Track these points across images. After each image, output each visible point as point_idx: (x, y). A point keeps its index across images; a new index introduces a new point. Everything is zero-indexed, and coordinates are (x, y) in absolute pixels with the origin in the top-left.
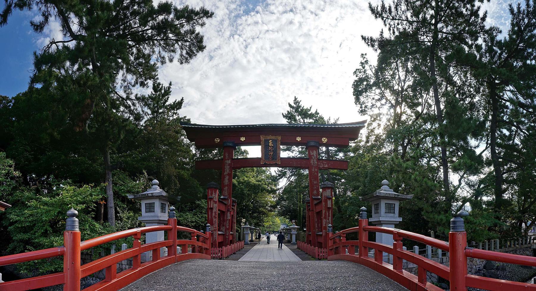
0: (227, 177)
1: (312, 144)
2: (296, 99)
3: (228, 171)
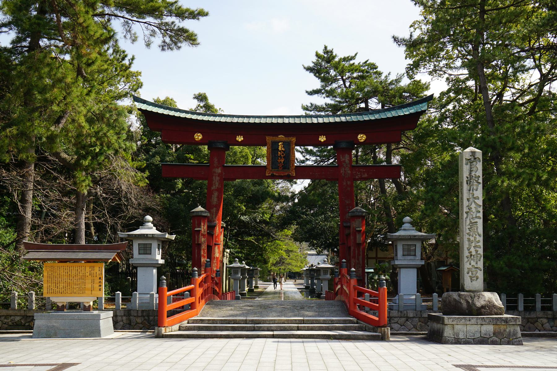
0: (216, 194)
1: (343, 145)
2: (326, 48)
3: (217, 184)
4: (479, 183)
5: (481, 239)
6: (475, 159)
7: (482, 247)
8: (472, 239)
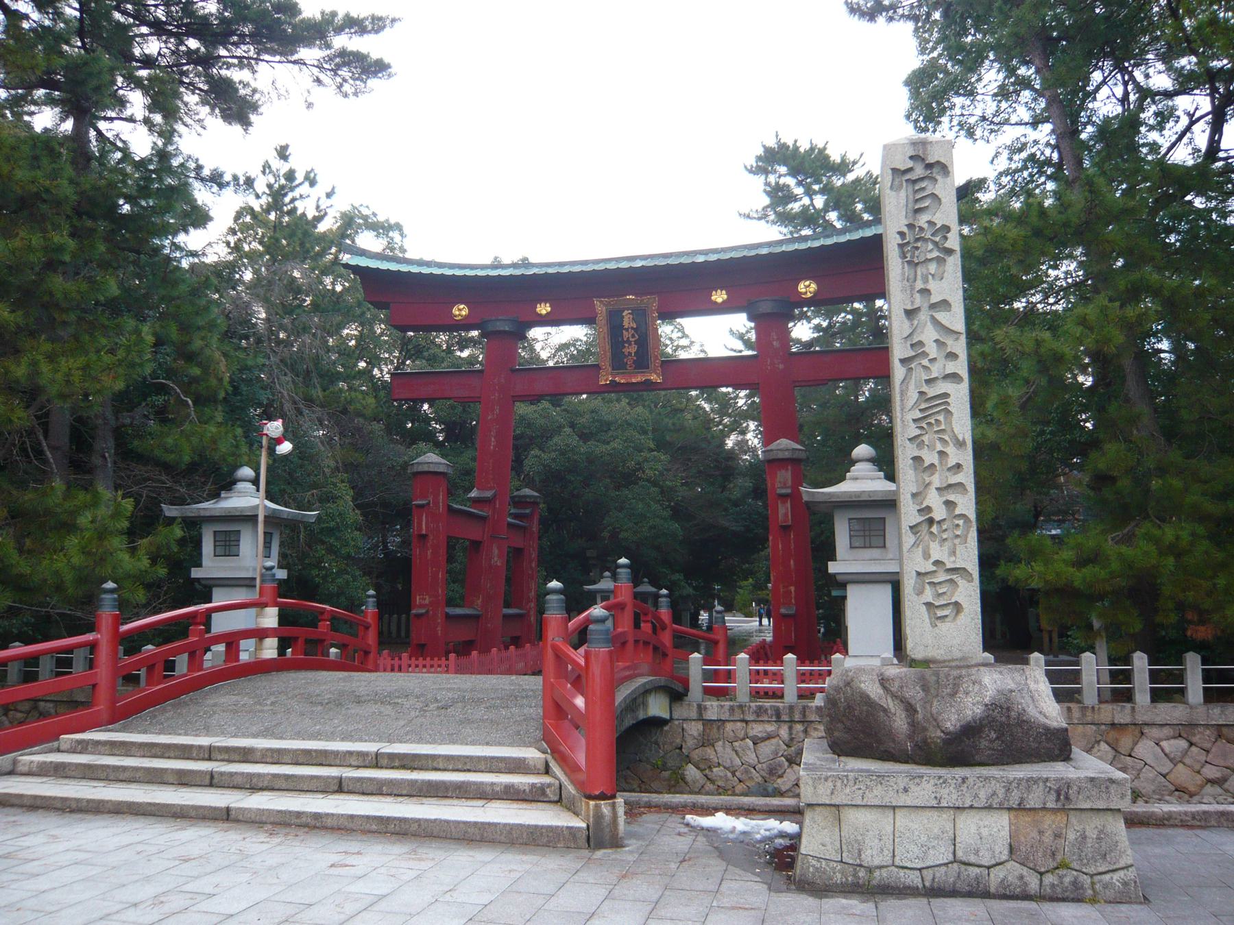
4: (950, 252)
5: (966, 458)
6: (929, 166)
7: (971, 488)
8: (930, 458)
